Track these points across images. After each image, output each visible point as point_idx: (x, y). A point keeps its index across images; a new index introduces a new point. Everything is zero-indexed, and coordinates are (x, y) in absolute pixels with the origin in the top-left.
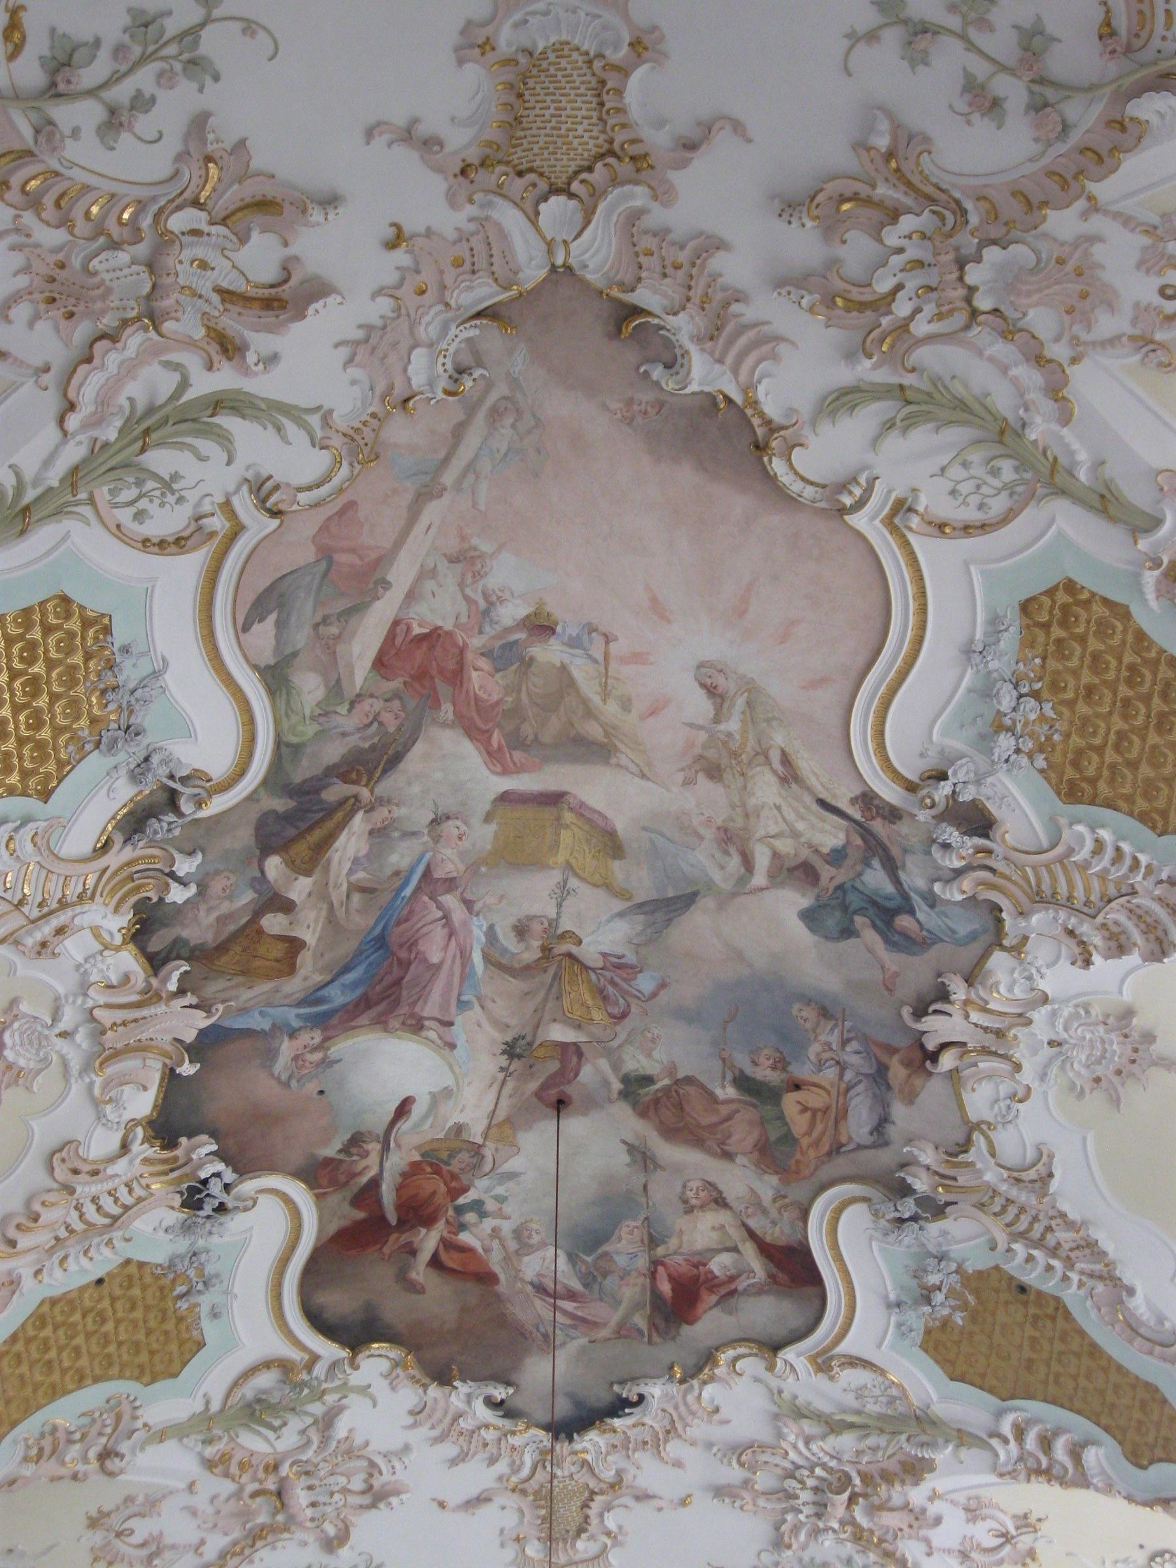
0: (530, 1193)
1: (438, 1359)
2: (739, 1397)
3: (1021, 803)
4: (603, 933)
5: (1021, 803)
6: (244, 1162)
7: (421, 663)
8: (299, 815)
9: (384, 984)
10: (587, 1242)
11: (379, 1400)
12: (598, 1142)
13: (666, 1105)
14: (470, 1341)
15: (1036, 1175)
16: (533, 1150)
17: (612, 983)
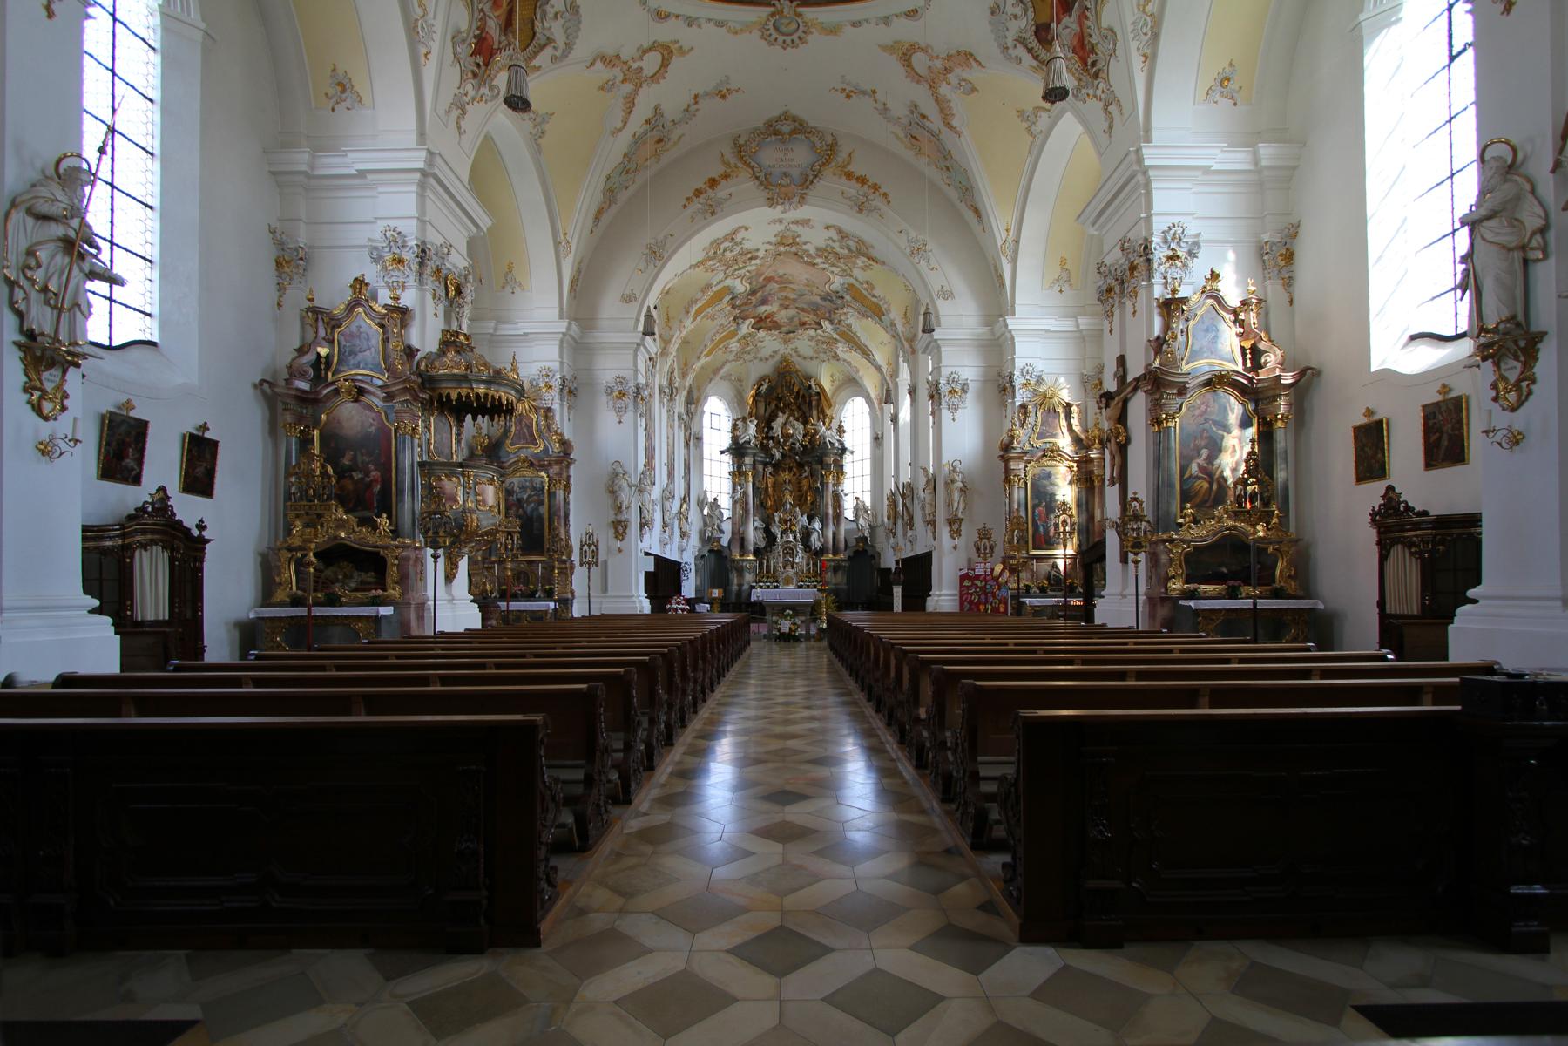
0: (782, 316)
1: (769, 329)
2: (812, 332)
3: (848, 298)
4: (792, 296)
5: (848, 298)
6: (744, 319)
7: (769, 280)
8: (753, 292)
9: (764, 302)
10: (791, 319)
11: (762, 333)
12: (792, 312)
13: (803, 310)
14: (776, 326)
15: (849, 326)
16: (783, 312)
17: (794, 300)
